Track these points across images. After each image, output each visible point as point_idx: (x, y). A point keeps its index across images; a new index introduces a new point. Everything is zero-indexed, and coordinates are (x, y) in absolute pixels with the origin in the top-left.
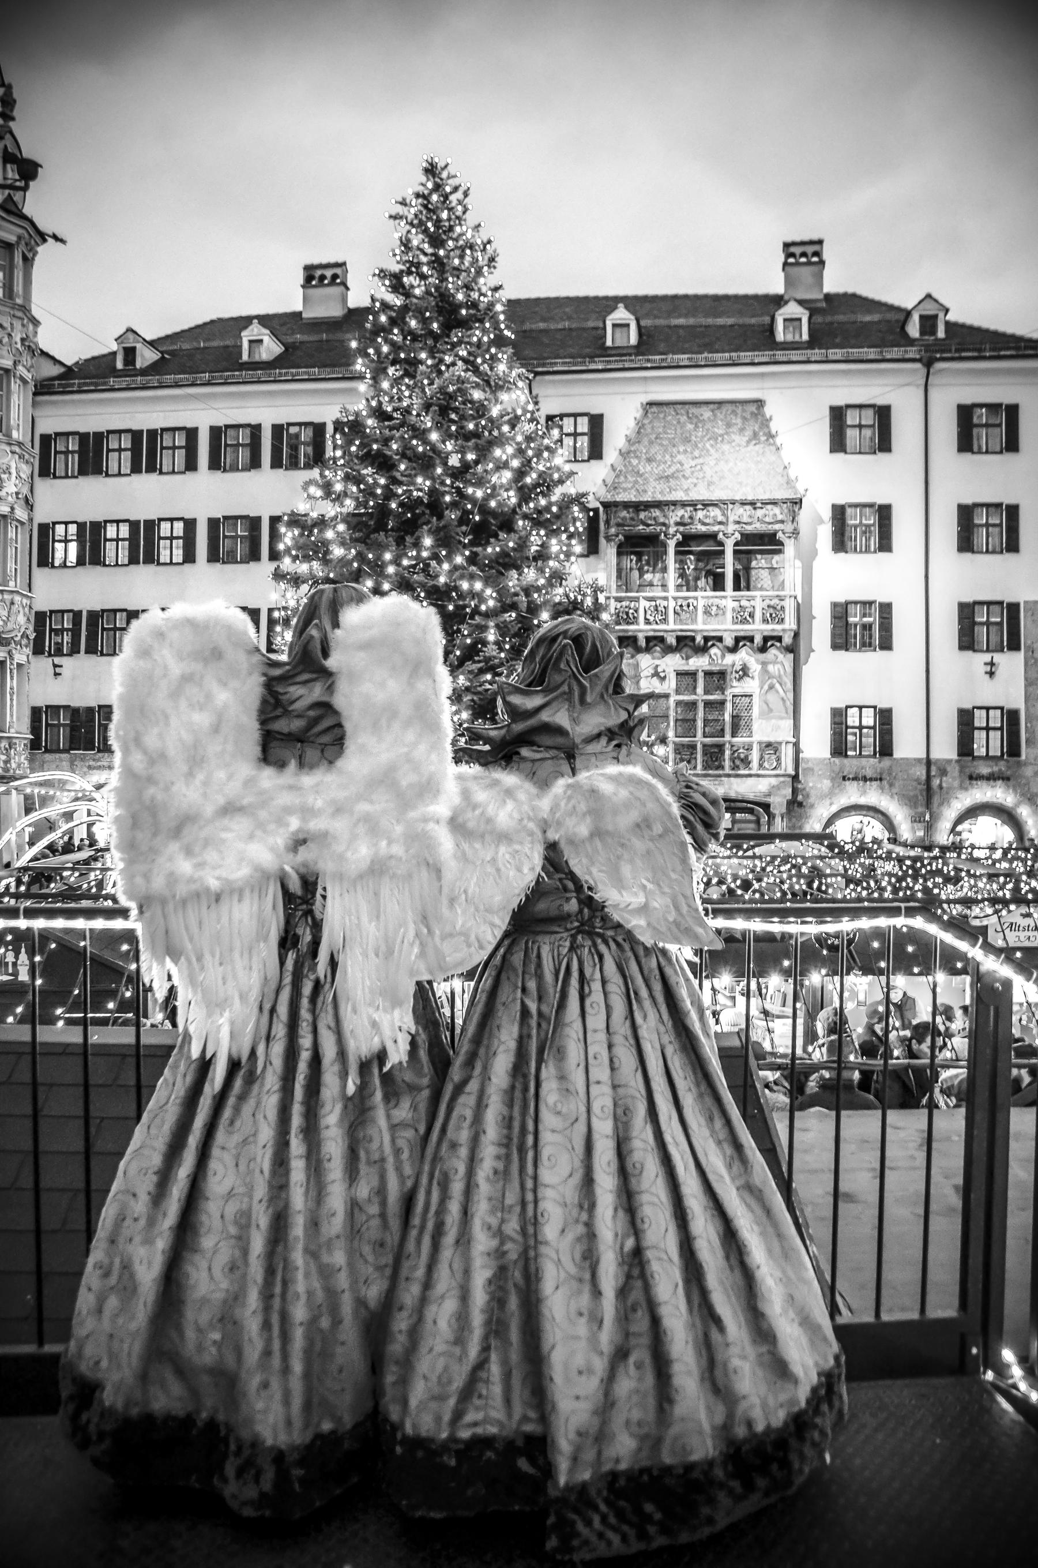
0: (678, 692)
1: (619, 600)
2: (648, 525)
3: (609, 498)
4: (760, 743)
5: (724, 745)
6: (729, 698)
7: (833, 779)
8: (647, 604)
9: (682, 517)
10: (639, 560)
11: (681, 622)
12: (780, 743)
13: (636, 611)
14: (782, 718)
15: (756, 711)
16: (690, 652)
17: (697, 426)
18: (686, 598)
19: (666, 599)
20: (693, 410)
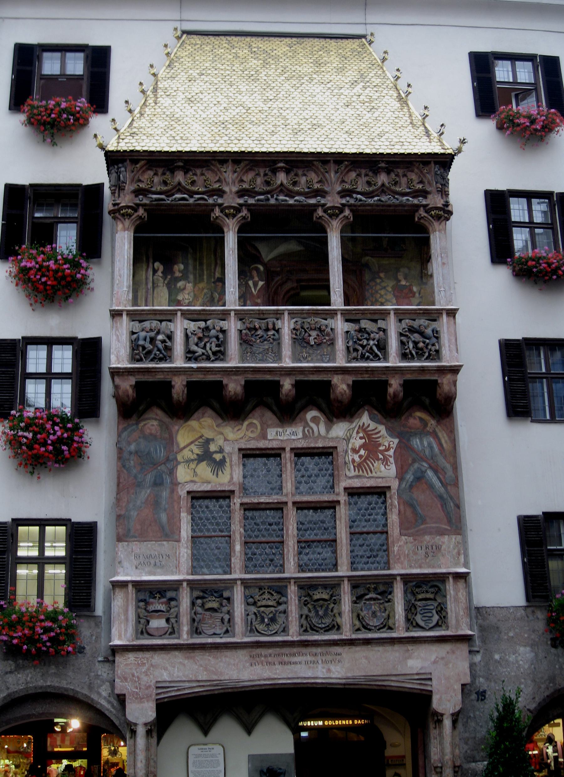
0: (244, 489)
1: (133, 316)
2: (191, 194)
3: (123, 146)
4: (407, 579)
5: (339, 585)
6: (343, 498)
7: (533, 645)
8: (192, 326)
9: (253, 180)
10: (168, 270)
11: (254, 357)
12: (442, 578)
13: (170, 337)
14: (442, 533)
15: (394, 518)
16: (269, 415)
17: (265, 64)
18: (261, 315)
19: (224, 315)
20: (257, 43)
